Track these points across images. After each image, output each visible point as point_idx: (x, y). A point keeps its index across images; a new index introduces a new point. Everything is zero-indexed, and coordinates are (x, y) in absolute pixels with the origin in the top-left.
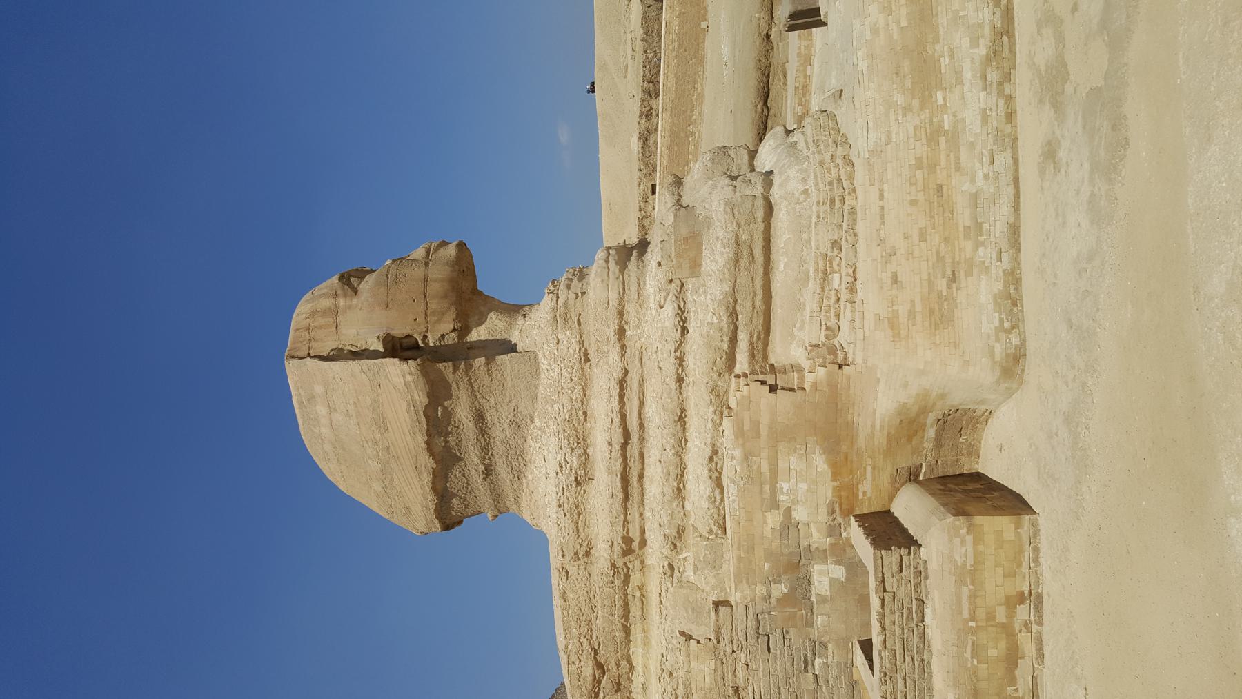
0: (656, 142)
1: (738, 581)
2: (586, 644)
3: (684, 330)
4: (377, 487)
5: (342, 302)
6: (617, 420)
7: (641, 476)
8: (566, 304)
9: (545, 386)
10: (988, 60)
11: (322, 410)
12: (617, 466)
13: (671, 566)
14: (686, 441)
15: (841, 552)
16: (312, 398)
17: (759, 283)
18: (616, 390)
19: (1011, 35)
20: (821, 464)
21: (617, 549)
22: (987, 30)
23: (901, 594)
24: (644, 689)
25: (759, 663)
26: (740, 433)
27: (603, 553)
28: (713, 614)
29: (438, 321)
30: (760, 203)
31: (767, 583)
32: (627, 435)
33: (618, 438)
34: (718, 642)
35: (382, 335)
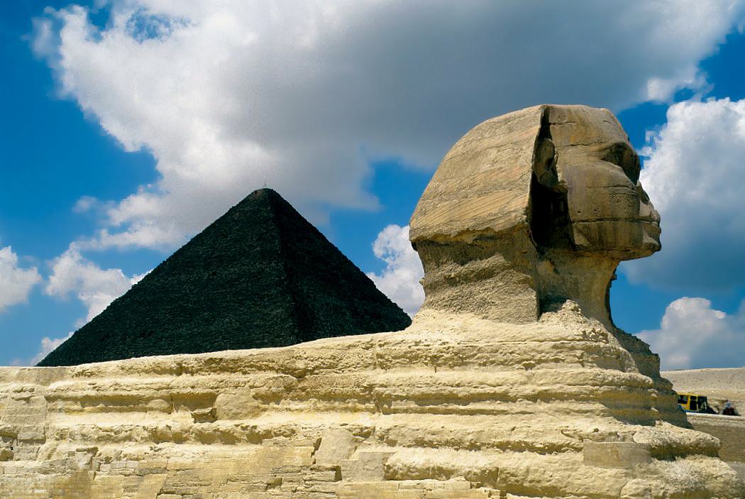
2: (317, 363)
3: (542, 451)
4: (442, 188)
5: (595, 148)
6: (473, 391)
7: (435, 412)
8: (573, 348)
11: (501, 138)
13: (367, 436)
14: (457, 450)
16: (511, 130)
18: (497, 390)
21: (382, 389)
27: (378, 376)
28: (329, 466)
33: (461, 392)
34: (311, 469)
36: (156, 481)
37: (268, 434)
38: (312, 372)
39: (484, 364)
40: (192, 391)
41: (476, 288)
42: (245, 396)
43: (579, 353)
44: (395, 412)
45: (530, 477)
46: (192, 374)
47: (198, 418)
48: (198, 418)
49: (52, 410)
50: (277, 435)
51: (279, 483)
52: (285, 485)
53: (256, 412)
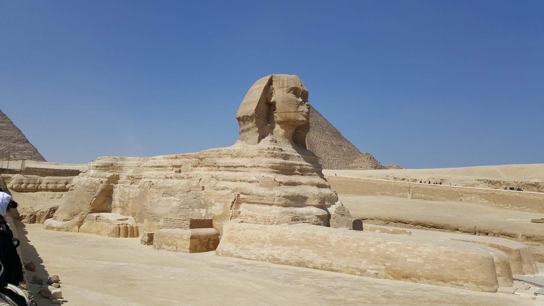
0: (533, 190)
1: (205, 192)
3: (249, 182)
5: (285, 89)
9: (250, 146)
10: (274, 257)
12: (230, 165)
17: (255, 201)
19: (278, 263)
20: (220, 213)
21: (217, 164)
22: (280, 258)
23: (183, 224)
25: (193, 196)
26: (228, 194)
30: (272, 202)
31: (204, 199)
32: (235, 167)
33: (235, 165)
41: (246, 134)
48: (176, 172)
52: (192, 192)
53: (192, 170)
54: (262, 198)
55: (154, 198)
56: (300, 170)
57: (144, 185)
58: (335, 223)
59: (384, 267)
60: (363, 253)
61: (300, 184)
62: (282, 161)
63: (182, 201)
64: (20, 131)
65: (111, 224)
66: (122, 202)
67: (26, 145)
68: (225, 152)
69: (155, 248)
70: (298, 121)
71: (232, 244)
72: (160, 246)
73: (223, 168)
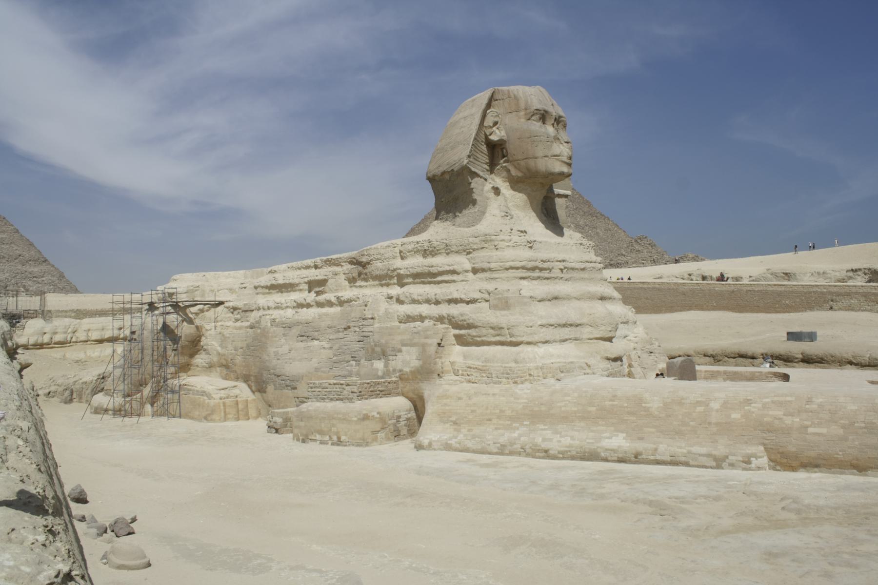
3: (468, 303)
5: (522, 113)
6: (440, 269)
7: (424, 283)
8: (491, 240)
11: (466, 113)
15: (387, 373)
16: (473, 106)
18: (451, 268)
23: (345, 392)
24: (360, 287)
26: (426, 330)
29: (515, 167)
30: (519, 339)
33: (434, 270)
35: (505, 138)
36: (296, 331)
37: (349, 301)
38: (368, 263)
39: (448, 254)
40: (317, 278)
42: (342, 280)
43: (496, 243)
44: (406, 284)
45: (461, 318)
46: (321, 267)
47: (318, 293)
49: (257, 294)
50: (351, 301)
51: (349, 327)
52: (352, 329)
54: (499, 332)
55: (281, 346)
56: (562, 270)
57: (258, 322)
58: (639, 369)
59: (762, 448)
60: (717, 424)
61: (568, 298)
62: (527, 254)
63: (336, 347)
64: (31, 244)
65: (209, 396)
66: (224, 355)
67: (44, 267)
68: (410, 247)
69: (298, 440)
70: (552, 174)
71: (447, 426)
72: (307, 436)
73: (410, 280)
